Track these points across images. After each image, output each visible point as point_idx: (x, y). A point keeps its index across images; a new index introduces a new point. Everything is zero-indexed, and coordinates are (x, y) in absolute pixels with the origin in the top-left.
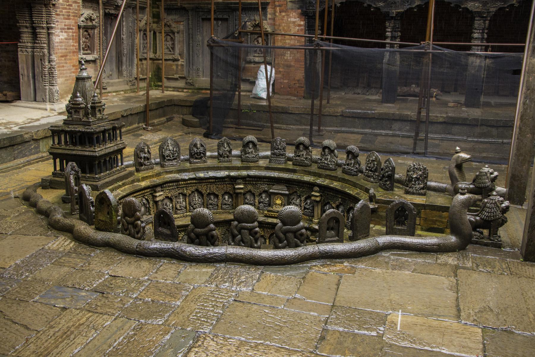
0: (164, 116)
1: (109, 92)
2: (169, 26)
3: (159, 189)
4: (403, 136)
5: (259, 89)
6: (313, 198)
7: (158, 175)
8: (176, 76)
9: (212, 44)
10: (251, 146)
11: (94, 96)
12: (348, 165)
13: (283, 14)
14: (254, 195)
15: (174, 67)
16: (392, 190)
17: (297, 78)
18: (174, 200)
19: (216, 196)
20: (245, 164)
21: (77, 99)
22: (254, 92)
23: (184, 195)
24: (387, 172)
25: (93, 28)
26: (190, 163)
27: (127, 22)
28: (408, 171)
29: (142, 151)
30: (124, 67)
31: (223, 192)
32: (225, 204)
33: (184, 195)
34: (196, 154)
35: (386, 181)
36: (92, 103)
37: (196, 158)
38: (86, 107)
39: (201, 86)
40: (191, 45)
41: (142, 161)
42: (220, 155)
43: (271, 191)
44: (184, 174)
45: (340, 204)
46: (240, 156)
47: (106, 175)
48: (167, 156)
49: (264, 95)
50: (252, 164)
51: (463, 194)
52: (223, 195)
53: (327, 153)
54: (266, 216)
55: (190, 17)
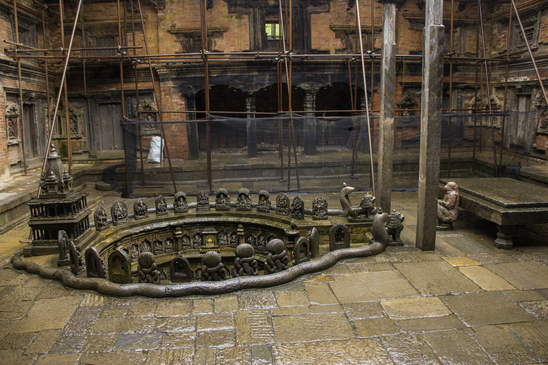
0: (80, 184)
1: (30, 169)
2: (71, 111)
3: (119, 243)
4: (272, 180)
5: (153, 156)
6: (238, 233)
7: (116, 232)
8: (80, 151)
9: (125, 123)
10: (182, 200)
11: (65, 173)
12: (261, 205)
13: (168, 97)
14: (189, 238)
15: (78, 144)
16: (303, 219)
17: (182, 145)
18: (130, 251)
19: (160, 243)
20: (178, 215)
21: (52, 177)
22: (149, 158)
23: (137, 246)
24: (298, 206)
25: (16, 116)
26: (136, 219)
27: (38, 110)
28: (313, 204)
29: (101, 214)
30: (38, 147)
31: (165, 239)
32: (168, 248)
33: (137, 246)
34: (139, 212)
35: (298, 213)
36: (64, 179)
37: (141, 215)
38: (60, 181)
39: (103, 157)
40: (91, 125)
41: (102, 222)
42: (158, 210)
43: (203, 232)
44: (134, 229)
45: (261, 235)
46: (174, 209)
47: (81, 238)
48: (119, 216)
49: (158, 160)
50: (184, 214)
51: (380, 213)
52: (165, 241)
53: (243, 198)
54: (202, 253)
55: (89, 103)
